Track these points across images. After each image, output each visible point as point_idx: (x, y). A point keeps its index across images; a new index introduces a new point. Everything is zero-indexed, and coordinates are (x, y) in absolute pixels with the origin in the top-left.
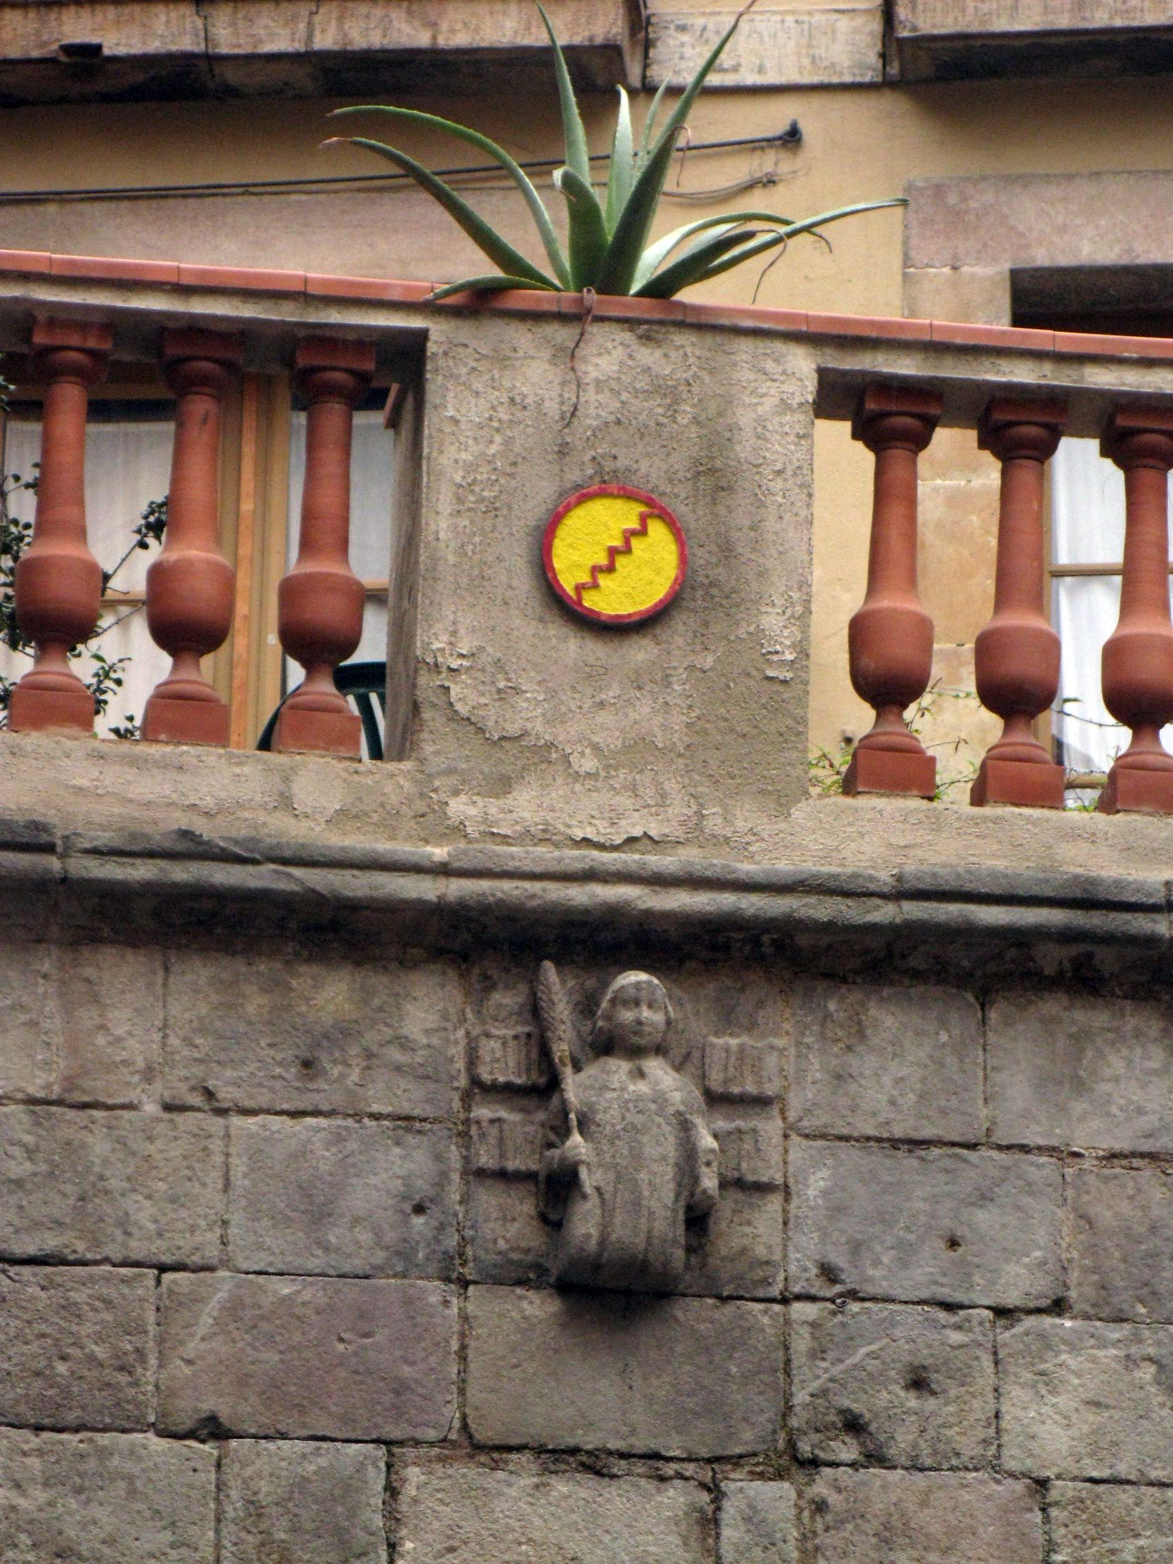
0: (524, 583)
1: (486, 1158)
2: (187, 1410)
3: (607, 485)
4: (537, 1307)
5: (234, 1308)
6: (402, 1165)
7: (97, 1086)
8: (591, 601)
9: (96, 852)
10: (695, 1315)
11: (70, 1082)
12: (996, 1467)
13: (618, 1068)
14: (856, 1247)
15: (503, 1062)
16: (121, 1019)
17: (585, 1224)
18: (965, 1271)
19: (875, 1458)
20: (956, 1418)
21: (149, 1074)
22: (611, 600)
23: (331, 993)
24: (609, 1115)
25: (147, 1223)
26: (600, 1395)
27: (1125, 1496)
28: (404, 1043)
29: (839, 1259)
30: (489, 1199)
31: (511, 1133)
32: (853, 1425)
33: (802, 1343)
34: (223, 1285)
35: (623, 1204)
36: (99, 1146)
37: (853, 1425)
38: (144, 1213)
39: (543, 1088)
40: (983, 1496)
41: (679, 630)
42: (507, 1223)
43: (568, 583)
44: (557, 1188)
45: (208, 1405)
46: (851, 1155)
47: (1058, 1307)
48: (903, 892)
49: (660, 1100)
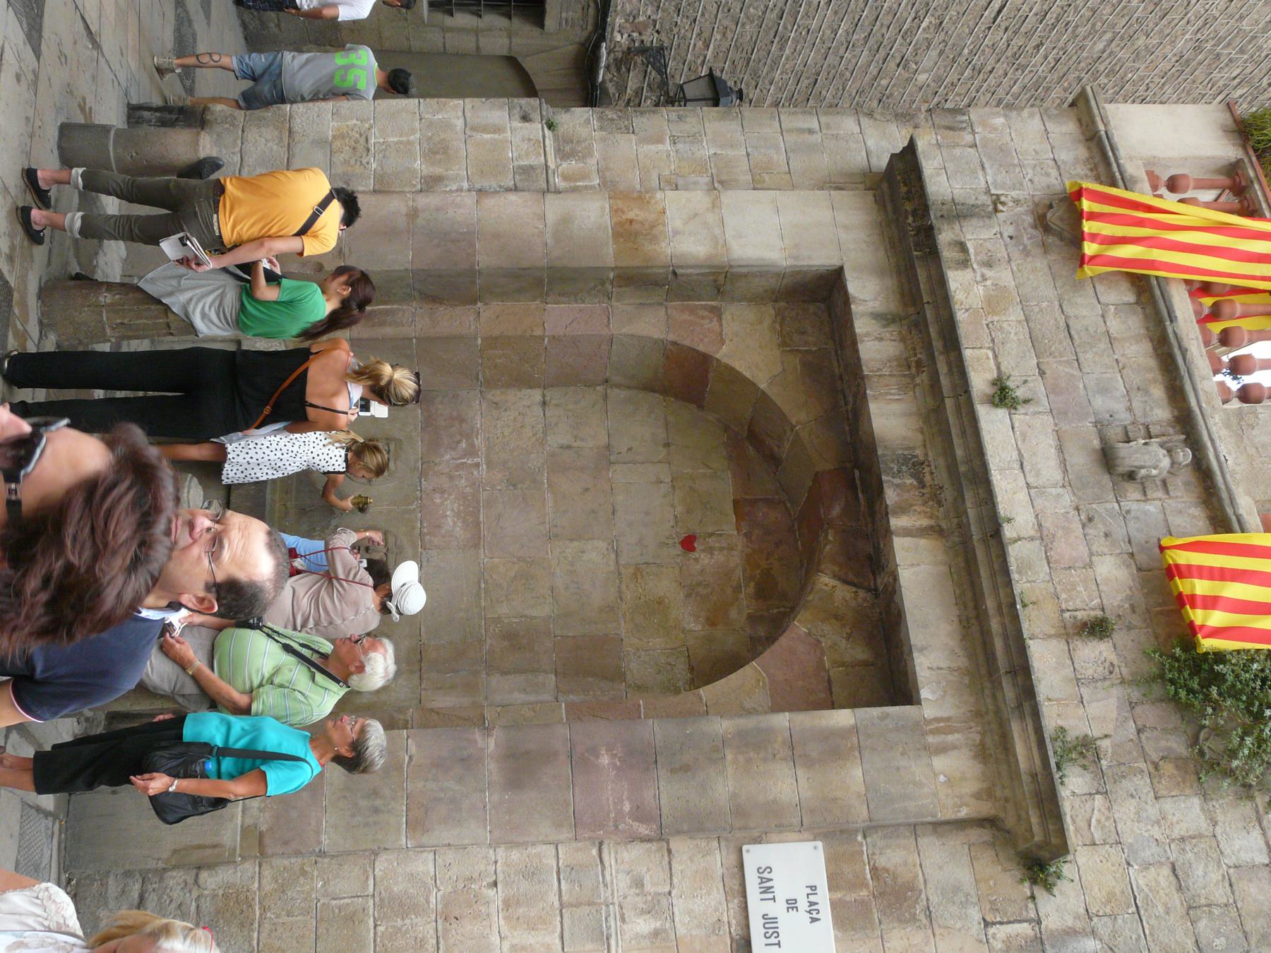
1: (1129, 428)
2: (1042, 367)
4: (1096, 443)
5: (1072, 376)
6: (1119, 407)
7: (1116, 345)
9: (1174, 332)
10: (1106, 479)
11: (1115, 339)
12: (1091, 554)
14: (1137, 518)
16: (1134, 348)
19: (1084, 526)
21: (1123, 355)
23: (1158, 392)
24: (1150, 448)
25: (1087, 357)
26: (1081, 460)
27: (1094, 587)
28: (1152, 409)
29: (1133, 514)
32: (1090, 520)
33: (1109, 506)
34: (1077, 373)
35: (1132, 455)
36: (1102, 346)
37: (1090, 520)
38: (1089, 356)
40: (1083, 550)
45: (1047, 371)
46: (1161, 516)
49: (1160, 461)
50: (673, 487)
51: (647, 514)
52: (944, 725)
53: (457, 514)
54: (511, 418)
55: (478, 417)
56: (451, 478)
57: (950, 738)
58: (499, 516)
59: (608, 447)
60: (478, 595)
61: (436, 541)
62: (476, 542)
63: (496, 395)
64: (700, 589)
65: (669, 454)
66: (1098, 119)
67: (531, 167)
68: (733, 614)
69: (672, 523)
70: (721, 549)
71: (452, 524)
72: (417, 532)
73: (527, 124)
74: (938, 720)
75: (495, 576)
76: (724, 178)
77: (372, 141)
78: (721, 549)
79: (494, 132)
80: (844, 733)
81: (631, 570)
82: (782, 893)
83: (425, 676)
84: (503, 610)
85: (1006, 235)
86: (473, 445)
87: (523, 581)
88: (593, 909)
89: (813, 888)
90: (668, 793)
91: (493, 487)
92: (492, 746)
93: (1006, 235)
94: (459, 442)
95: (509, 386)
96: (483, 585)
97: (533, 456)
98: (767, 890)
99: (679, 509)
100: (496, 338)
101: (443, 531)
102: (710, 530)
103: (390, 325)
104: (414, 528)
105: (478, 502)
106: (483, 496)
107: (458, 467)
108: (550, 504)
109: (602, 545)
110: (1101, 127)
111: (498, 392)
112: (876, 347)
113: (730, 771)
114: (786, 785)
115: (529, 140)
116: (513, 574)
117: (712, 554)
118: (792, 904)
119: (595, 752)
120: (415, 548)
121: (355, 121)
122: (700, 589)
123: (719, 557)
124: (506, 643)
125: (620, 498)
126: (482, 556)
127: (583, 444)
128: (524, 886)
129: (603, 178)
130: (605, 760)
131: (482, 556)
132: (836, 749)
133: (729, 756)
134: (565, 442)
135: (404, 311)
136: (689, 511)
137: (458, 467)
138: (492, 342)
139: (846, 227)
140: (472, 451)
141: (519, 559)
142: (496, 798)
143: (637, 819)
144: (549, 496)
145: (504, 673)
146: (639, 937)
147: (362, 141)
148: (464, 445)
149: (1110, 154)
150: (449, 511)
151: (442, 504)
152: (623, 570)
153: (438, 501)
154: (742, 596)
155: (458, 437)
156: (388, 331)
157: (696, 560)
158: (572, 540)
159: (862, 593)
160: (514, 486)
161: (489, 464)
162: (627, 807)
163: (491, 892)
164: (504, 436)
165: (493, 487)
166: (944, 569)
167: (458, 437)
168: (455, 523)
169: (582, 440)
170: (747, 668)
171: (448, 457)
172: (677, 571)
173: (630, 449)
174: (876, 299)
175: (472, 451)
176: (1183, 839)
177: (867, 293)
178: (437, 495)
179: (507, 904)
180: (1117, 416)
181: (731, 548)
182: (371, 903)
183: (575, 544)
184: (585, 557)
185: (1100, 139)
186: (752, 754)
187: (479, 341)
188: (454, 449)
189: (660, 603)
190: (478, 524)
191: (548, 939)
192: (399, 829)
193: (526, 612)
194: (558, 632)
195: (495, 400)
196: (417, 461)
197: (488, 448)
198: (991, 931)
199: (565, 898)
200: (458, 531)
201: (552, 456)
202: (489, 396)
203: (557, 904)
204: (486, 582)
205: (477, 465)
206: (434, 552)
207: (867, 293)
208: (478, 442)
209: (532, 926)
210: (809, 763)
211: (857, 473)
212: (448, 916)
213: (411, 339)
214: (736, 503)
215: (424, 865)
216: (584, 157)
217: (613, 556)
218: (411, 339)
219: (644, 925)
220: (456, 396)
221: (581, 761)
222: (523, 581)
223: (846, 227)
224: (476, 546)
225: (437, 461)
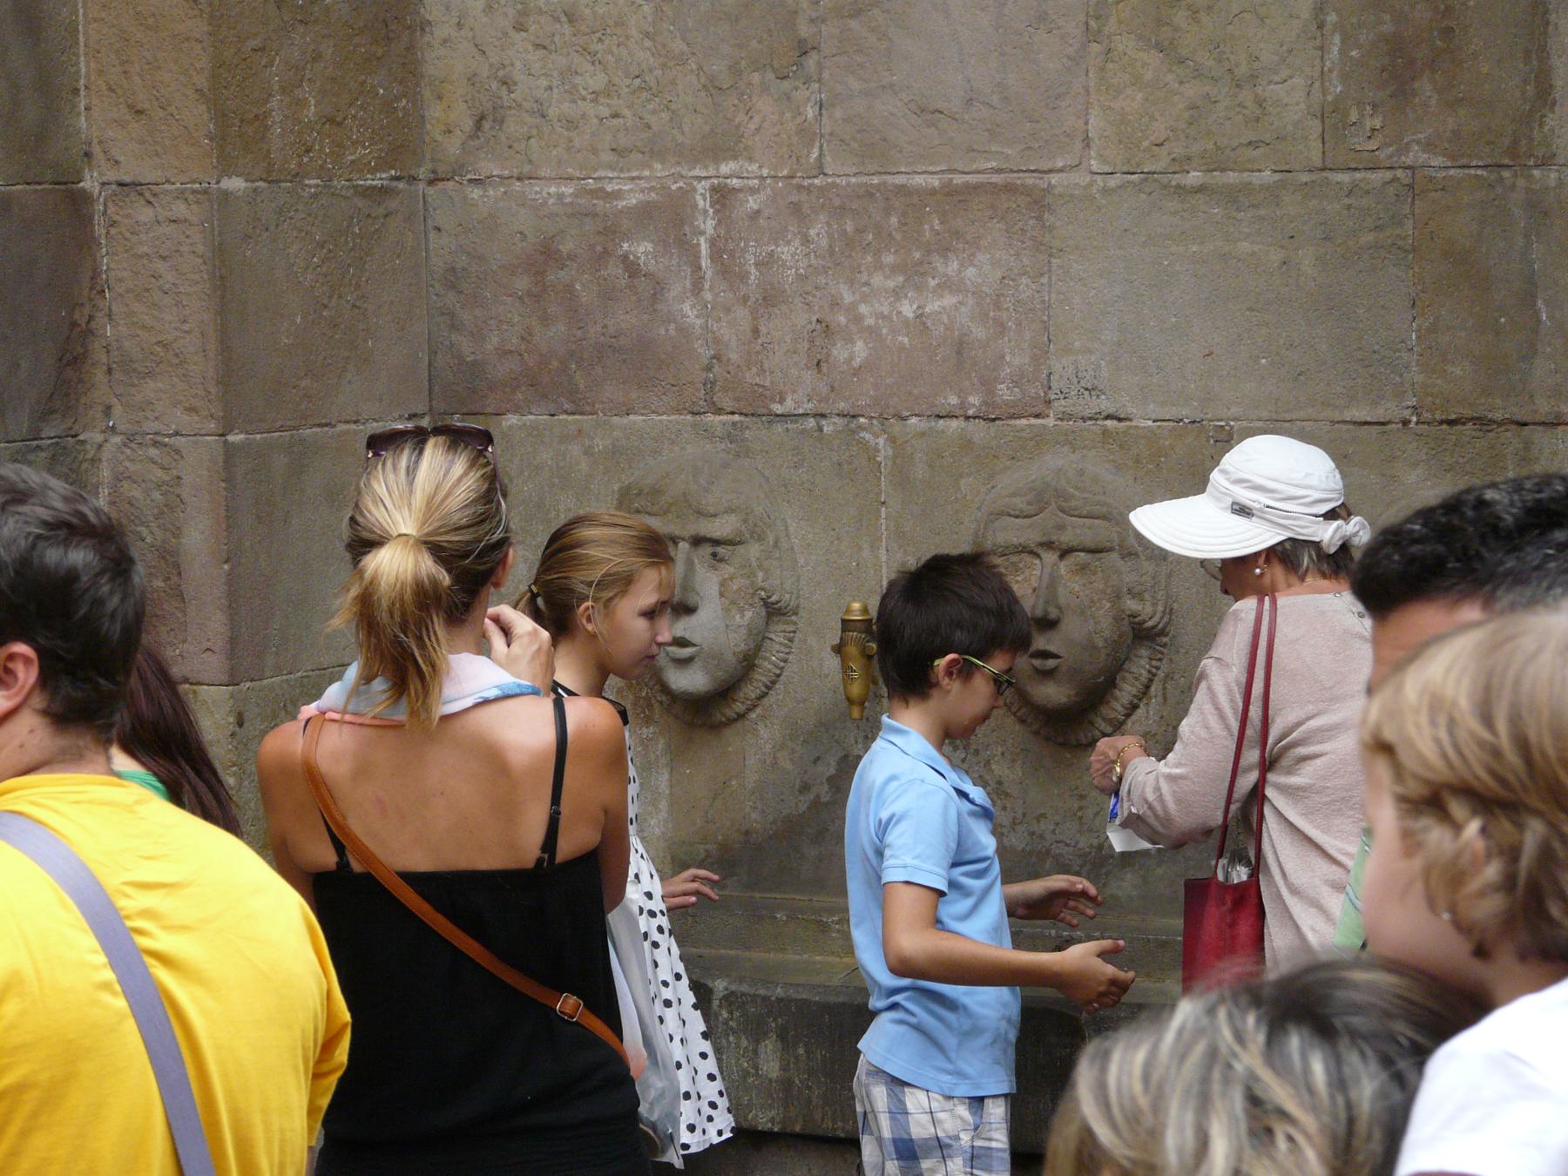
53: (914, 275)
54: (535, 57)
55: (535, 190)
56: (771, 299)
58: (927, 112)
60: (1233, 197)
61: (1016, 360)
63: (446, 119)
71: (950, 295)
72: (978, 430)
75: (1160, 130)
83: (1544, 408)
84: (1292, 98)
86: (645, 213)
87: (1180, 17)
91: (807, 135)
95: (410, 72)
96: (1194, 177)
100: (221, 116)
101: (979, 332)
103: (177, 533)
104: (967, 444)
106: (843, 173)
107: (729, 271)
111: (435, 112)
116: (1153, 58)
120: (1040, 441)
124: (1425, 87)
126: (1082, 178)
131: (1082, 178)
135: (118, 478)
137: (729, 271)
138: (236, 132)
140: (668, 218)
141: (1092, 35)
145: (1544, 95)
148: (642, 249)
150: (896, 309)
151: (872, 332)
153: (860, 349)
155: (614, 270)
156: (198, 538)
160: (804, 49)
161: (715, 150)
164: (610, 90)
165: (807, 135)
167: (614, 270)
168: (947, 286)
171: (689, 311)
175: (668, 218)
178: (839, 353)
187: (235, 184)
188: (658, 288)
190: (950, 191)
195: (468, 124)
196: (708, 434)
197: (655, 151)
202: (453, 147)
204: (1182, 164)
205: (722, 196)
206: (1061, 367)
208: (631, 191)
213: (230, 452)
218: (230, 452)
220: (452, 279)
222: (1180, 17)
224: (1039, 202)
225: (705, 353)
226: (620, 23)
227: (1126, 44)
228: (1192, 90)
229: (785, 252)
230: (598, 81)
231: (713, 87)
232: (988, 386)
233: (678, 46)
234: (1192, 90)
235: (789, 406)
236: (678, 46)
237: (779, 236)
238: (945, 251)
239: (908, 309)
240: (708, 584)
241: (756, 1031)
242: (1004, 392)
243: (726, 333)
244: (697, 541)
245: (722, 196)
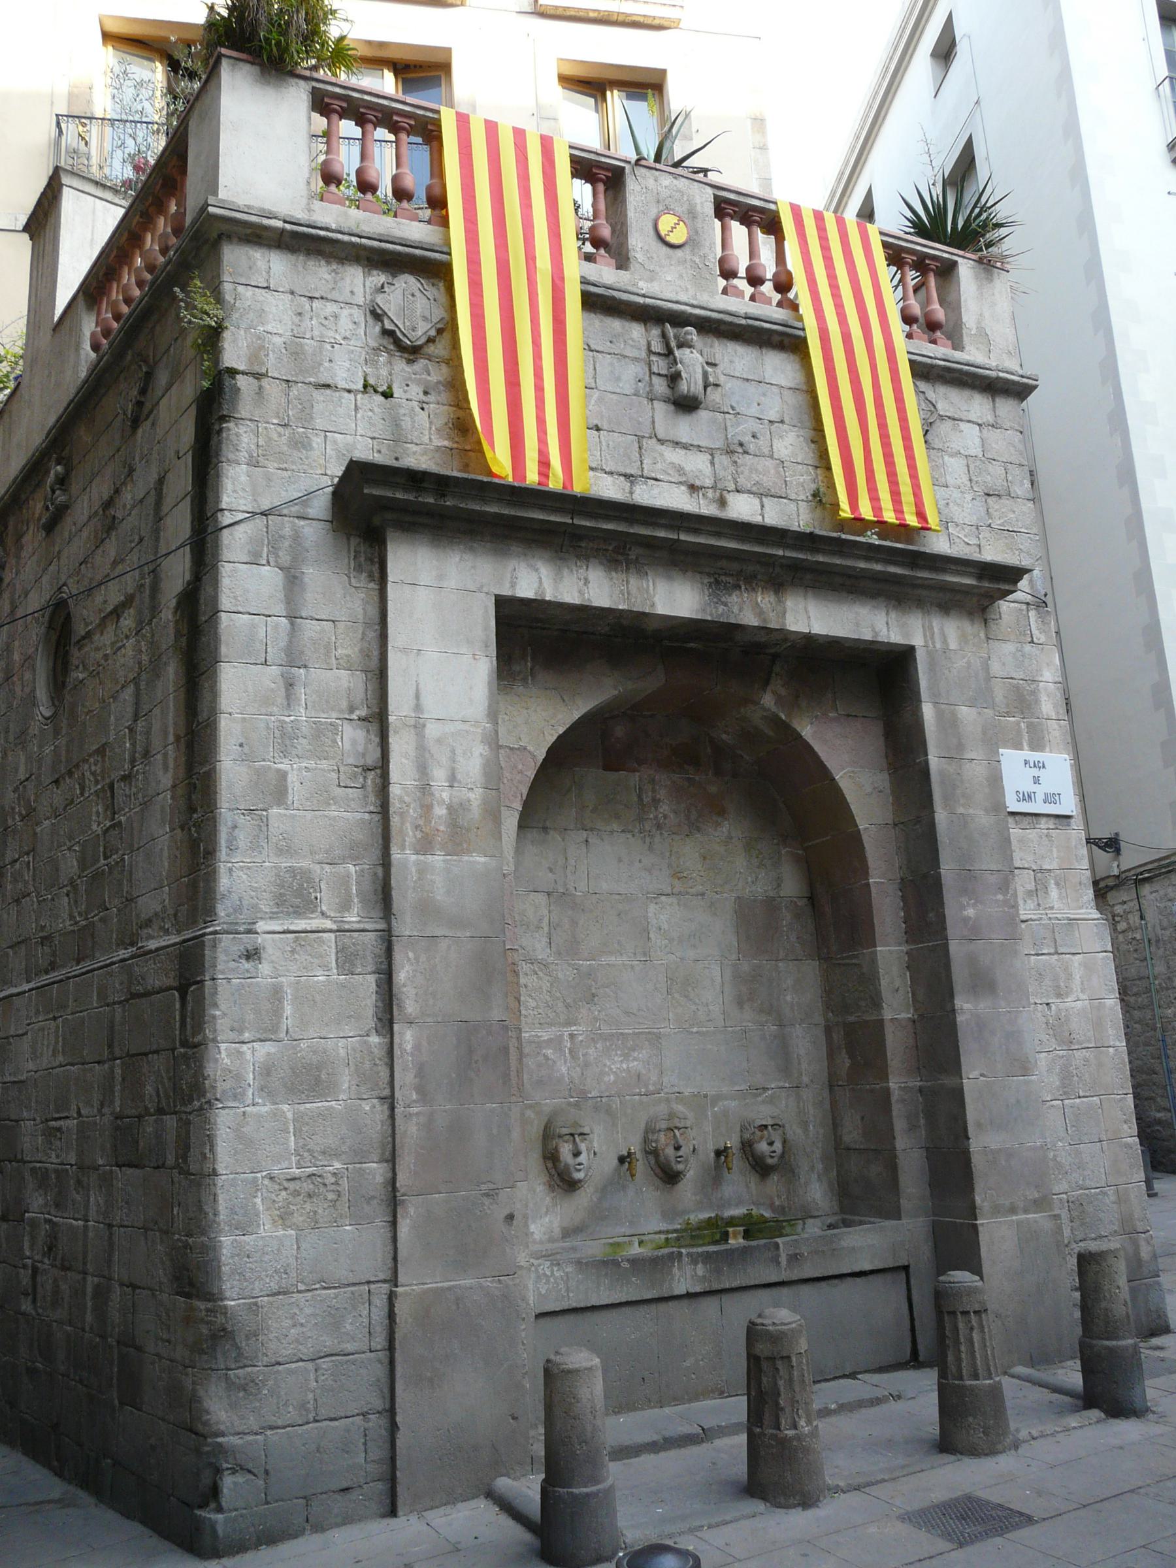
0: (652, 232)
3: (668, 210)
8: (668, 239)
12: (771, 457)
13: (687, 351)
15: (657, 346)
17: (683, 387)
18: (762, 411)
19: (746, 452)
20: (763, 442)
22: (672, 239)
30: (655, 379)
31: (660, 365)
32: (741, 445)
39: (669, 353)
40: (769, 463)
41: (687, 249)
42: (660, 386)
43: (663, 233)
44: (674, 378)
45: (595, 422)
47: (782, 422)
48: (747, 317)
50: (592, 830)
51: (620, 860)
52: (928, 632)
53: (626, 1057)
56: (587, 1065)
57: (936, 630)
59: (549, 894)
61: (654, 1078)
62: (655, 1039)
64: (693, 817)
65: (555, 829)
66: (266, 222)
67: (341, 950)
68: (713, 789)
69: (629, 836)
70: (654, 791)
73: (263, 955)
74: (925, 636)
76: (344, 704)
77: (296, 1172)
78: (654, 791)
79: (281, 1000)
80: (940, 715)
81: (676, 882)
82: (1029, 787)
85: (424, 398)
86: (550, 1041)
88: (1056, 929)
89: (1026, 762)
90: (987, 862)
92: (966, 1006)
93: (424, 398)
94: (546, 1058)
96: (695, 1030)
97: (560, 975)
98: (1030, 797)
99: (615, 826)
101: (644, 1072)
102: (636, 799)
105: (612, 1035)
106: (606, 1029)
108: (612, 959)
109: (652, 908)
110: (280, 224)
112: (590, 587)
113: (971, 811)
114: (975, 771)
115: (293, 951)
117: (659, 800)
118: (1036, 780)
119: (966, 920)
121: (258, 1200)
122: (693, 817)
123: (662, 794)
124: (746, 1006)
125: (605, 886)
127: (546, 920)
128: (1047, 982)
129: (344, 860)
130: (970, 912)
132: (950, 723)
133: (961, 810)
134: (545, 940)
136: (617, 817)
137: (574, 1057)
139: (440, 577)
140: (556, 1042)
142: (1003, 1003)
143: (1007, 889)
144: (604, 960)
146: (1060, 898)
147: (292, 1186)
148: (549, 1052)
149: (322, 233)
152: (676, 890)
154: (697, 778)
155: (541, 1058)
157: (665, 817)
158: (649, 938)
159: (777, 669)
160: (594, 995)
161: (569, 1023)
162: (1000, 897)
163: (1053, 1007)
164: (537, 1007)
165: (596, 1019)
166: (810, 594)
167: (541, 1058)
168: (635, 1059)
169: (540, 920)
170: (841, 784)
172: (677, 838)
173: (551, 870)
174: (537, 570)
176: (970, 480)
177: (535, 579)
179: (1059, 995)
180: (640, 376)
181: (653, 781)
182: (1066, 1102)
183: (652, 935)
184: (665, 926)
185: (295, 234)
186: (958, 792)
189: (705, 858)
190: (634, 1033)
191: (1076, 965)
192: (1027, 1083)
193: (718, 987)
194: (734, 956)
197: (551, 1025)
198: (1035, 640)
199: (1052, 951)
200: (643, 1054)
201: (560, 954)
203: (1056, 957)
204: (692, 1026)
205: (572, 1036)
206: (665, 1080)
207: (535, 579)
208: (545, 1036)
209: (1070, 976)
210: (960, 747)
211: (666, 643)
212: (1068, 1042)
214: (607, 767)
215: (1043, 1060)
216: (309, 880)
217: (663, 898)
219: (1054, 893)
221: (974, 934)
223: (440, 577)
224: (658, 1037)
226: (541, 988)
227: (676, 995)
228: (694, 1007)
229: (590, 1051)
230: (534, 1004)
231: (567, 1006)
232: (646, 1086)
233: (558, 994)
234: (694, 1007)
235: (593, 1094)
236: (558, 994)
237: (587, 1048)
238: (634, 1050)
239: (625, 1066)
240: (583, 1147)
241: (696, 1264)
242: (651, 1088)
243: (573, 1074)
244: (581, 1134)
245: (572, 1036)
